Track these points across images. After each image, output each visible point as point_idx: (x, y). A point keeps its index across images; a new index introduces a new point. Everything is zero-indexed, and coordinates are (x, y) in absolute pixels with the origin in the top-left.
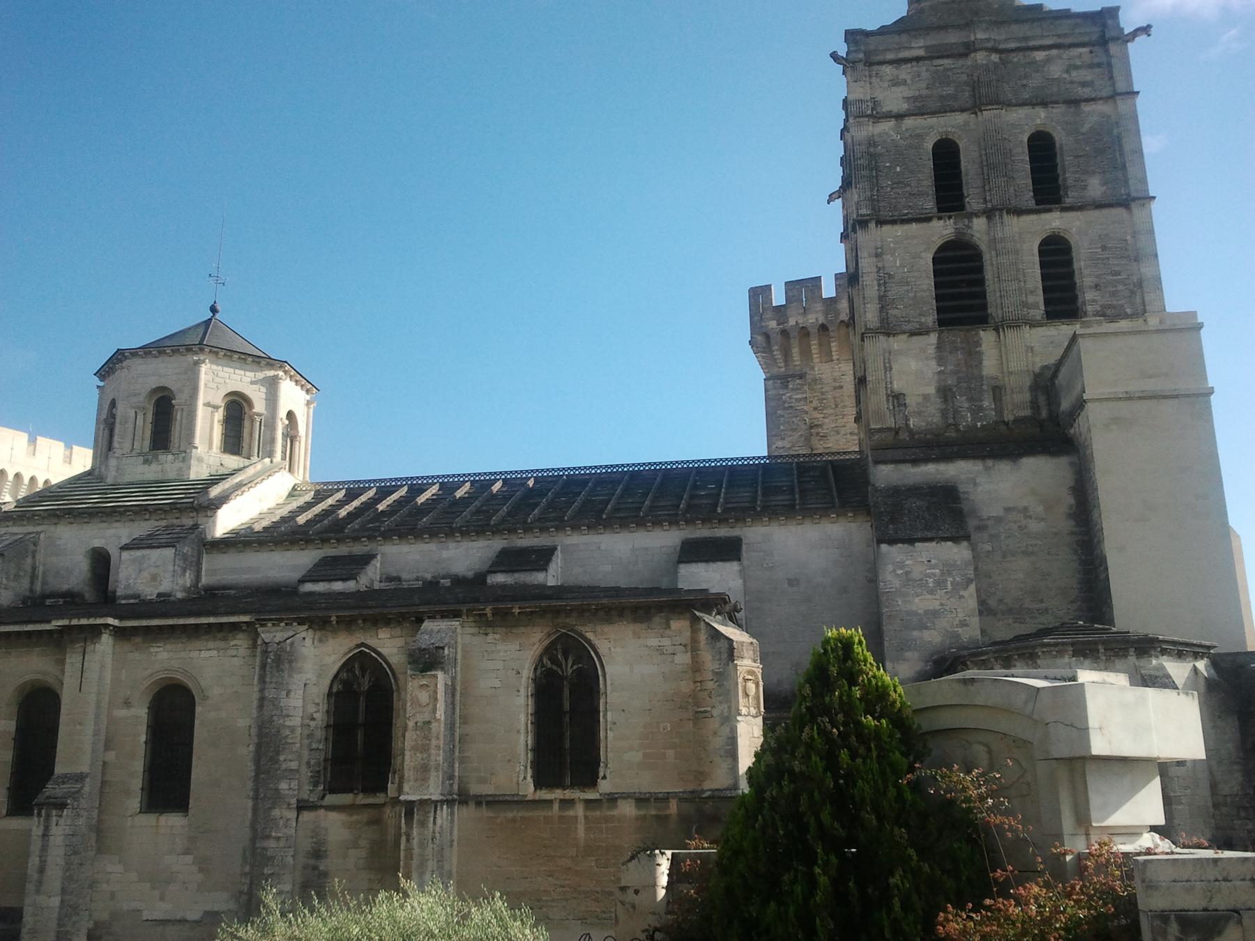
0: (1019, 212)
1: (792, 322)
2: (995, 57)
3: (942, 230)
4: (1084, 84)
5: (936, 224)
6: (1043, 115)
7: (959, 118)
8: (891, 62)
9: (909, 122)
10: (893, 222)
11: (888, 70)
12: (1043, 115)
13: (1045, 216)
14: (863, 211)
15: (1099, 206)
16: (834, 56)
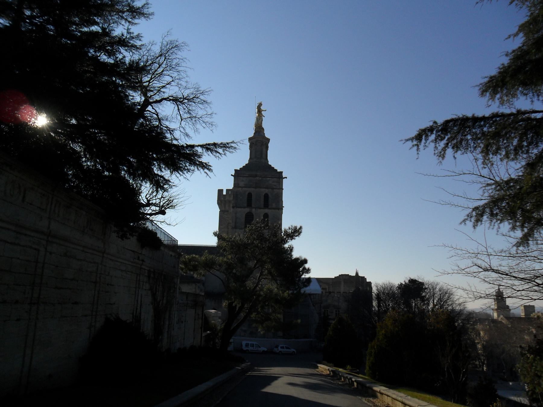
0: (260, 208)
1: (227, 199)
2: (260, 178)
3: (247, 210)
4: (275, 186)
5: (246, 209)
6: (267, 191)
7: (253, 189)
8: (242, 177)
9: (244, 189)
10: (239, 208)
11: (241, 178)
12: (267, 191)
13: (265, 210)
14: (234, 205)
15: (274, 209)
16: (232, 175)
